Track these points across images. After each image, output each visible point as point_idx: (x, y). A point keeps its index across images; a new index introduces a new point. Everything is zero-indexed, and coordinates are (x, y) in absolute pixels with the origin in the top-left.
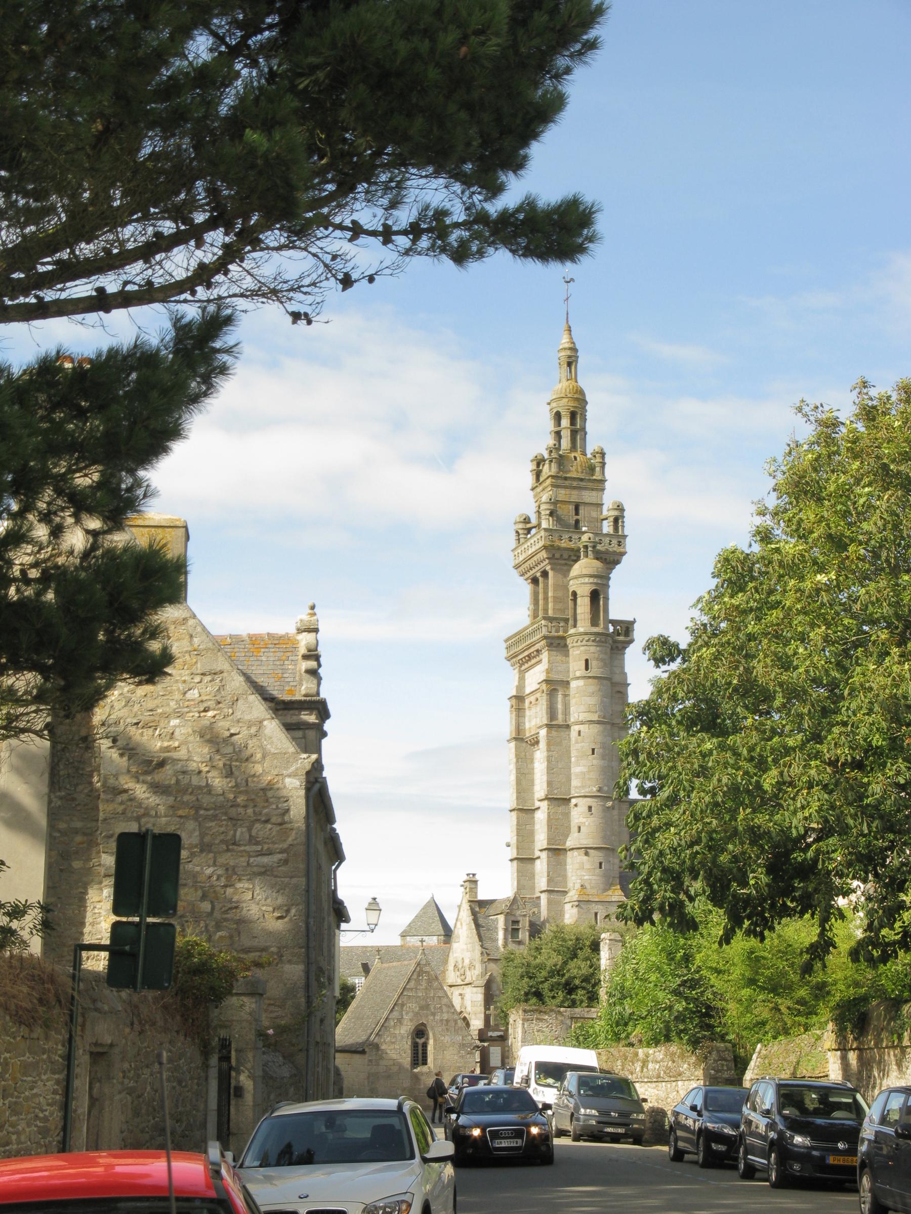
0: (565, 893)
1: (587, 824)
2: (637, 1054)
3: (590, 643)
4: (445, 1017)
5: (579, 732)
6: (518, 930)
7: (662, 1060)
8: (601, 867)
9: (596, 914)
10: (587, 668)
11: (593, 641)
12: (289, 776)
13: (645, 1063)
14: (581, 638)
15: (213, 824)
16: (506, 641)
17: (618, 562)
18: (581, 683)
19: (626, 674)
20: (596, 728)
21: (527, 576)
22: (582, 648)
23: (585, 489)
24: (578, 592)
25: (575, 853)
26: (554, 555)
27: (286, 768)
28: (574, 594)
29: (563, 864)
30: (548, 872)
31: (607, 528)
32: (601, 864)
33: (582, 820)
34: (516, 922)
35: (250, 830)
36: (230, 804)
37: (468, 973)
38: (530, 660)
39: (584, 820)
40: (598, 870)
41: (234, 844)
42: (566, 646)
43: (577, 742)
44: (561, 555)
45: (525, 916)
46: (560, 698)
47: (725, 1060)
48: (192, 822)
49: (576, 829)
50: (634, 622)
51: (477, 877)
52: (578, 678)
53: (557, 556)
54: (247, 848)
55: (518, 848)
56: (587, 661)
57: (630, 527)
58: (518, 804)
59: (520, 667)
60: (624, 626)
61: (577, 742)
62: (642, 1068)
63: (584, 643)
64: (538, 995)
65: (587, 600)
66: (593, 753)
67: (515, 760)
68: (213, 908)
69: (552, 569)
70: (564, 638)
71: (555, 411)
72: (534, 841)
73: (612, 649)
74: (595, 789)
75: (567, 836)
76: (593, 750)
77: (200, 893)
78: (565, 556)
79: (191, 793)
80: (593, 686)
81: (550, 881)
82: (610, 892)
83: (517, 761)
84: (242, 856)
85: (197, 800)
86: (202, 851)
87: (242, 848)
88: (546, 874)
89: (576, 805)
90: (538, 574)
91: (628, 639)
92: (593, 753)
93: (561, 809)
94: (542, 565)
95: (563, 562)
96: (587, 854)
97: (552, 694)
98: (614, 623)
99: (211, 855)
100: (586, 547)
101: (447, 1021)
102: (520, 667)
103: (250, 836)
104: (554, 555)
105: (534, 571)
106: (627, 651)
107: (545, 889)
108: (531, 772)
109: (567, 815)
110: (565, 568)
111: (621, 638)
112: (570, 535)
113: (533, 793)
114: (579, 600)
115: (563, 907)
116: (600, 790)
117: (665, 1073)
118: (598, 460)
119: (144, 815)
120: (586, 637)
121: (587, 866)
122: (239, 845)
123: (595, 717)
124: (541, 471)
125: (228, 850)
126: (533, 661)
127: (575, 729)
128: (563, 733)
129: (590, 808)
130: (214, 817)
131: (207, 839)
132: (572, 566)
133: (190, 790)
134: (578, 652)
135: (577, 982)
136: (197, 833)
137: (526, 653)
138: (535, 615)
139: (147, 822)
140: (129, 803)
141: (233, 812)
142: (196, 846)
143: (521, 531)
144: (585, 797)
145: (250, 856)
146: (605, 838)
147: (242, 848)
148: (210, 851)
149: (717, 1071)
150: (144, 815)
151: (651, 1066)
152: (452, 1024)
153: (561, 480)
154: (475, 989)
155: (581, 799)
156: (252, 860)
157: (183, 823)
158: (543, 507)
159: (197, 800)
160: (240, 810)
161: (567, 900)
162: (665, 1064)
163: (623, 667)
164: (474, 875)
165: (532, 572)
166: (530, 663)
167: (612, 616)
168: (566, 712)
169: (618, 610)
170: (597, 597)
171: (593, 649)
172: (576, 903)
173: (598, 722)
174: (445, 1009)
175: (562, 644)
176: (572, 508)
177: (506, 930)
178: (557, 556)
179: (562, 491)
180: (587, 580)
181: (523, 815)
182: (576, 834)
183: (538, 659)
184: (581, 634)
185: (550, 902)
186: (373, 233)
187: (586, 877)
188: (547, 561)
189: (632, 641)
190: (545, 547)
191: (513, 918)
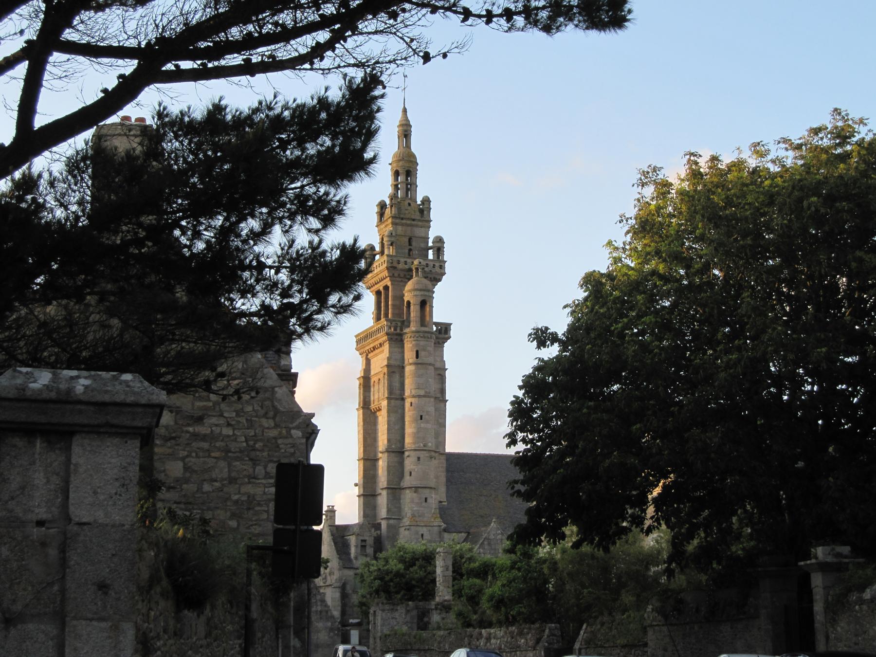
2: (481, 634)
4: (319, 608)
5: (411, 403)
7: (503, 637)
10: (417, 357)
12: (294, 428)
13: (488, 639)
15: (238, 463)
16: (356, 336)
17: (440, 280)
19: (444, 361)
21: (372, 289)
23: (417, 226)
24: (412, 302)
27: (292, 423)
28: (409, 303)
30: (388, 505)
31: (431, 256)
33: (412, 467)
35: (265, 467)
36: (251, 449)
37: (328, 578)
38: (374, 350)
39: (414, 467)
41: (255, 478)
44: (399, 275)
47: (555, 635)
48: (222, 462)
50: (450, 324)
51: (335, 508)
52: (411, 364)
53: (396, 275)
54: (263, 481)
56: (417, 352)
57: (448, 255)
60: (443, 327)
62: (486, 643)
64: (387, 592)
65: (418, 307)
68: (238, 525)
71: (395, 169)
73: (435, 343)
77: (228, 514)
78: (402, 275)
79: (222, 441)
84: (260, 487)
85: (227, 445)
86: (230, 483)
87: (260, 481)
89: (408, 456)
90: (381, 289)
91: (447, 336)
94: (385, 281)
95: (400, 279)
98: (437, 324)
99: (237, 486)
100: (417, 269)
101: (321, 612)
103: (266, 472)
106: (446, 344)
107: (385, 516)
110: (401, 284)
111: (442, 336)
112: (405, 260)
114: (412, 307)
117: (505, 646)
119: (187, 456)
121: (416, 500)
122: (258, 479)
124: (384, 213)
125: (249, 483)
126: (377, 351)
129: (419, 458)
130: (237, 459)
131: (233, 474)
132: (406, 283)
133: (221, 438)
135: (414, 582)
136: (226, 470)
137: (372, 345)
138: (378, 318)
139: (190, 461)
140: (176, 447)
141: (253, 454)
142: (225, 479)
144: (415, 450)
145: (265, 487)
147: (260, 481)
148: (236, 483)
149: (550, 644)
150: (187, 456)
151: (493, 641)
152: (324, 614)
153: (398, 219)
154: (334, 589)
155: (412, 452)
156: (267, 490)
157: (216, 463)
158: (385, 239)
159: (227, 445)
160: (258, 453)
162: (505, 640)
163: (443, 357)
164: (333, 506)
165: (376, 286)
166: (374, 352)
167: (434, 320)
169: (439, 315)
170: (425, 304)
174: (319, 603)
176: (407, 240)
177: (356, 546)
179: (400, 228)
183: (381, 349)
184: (413, 332)
186: (479, 16)
187: (415, 509)
189: (449, 338)
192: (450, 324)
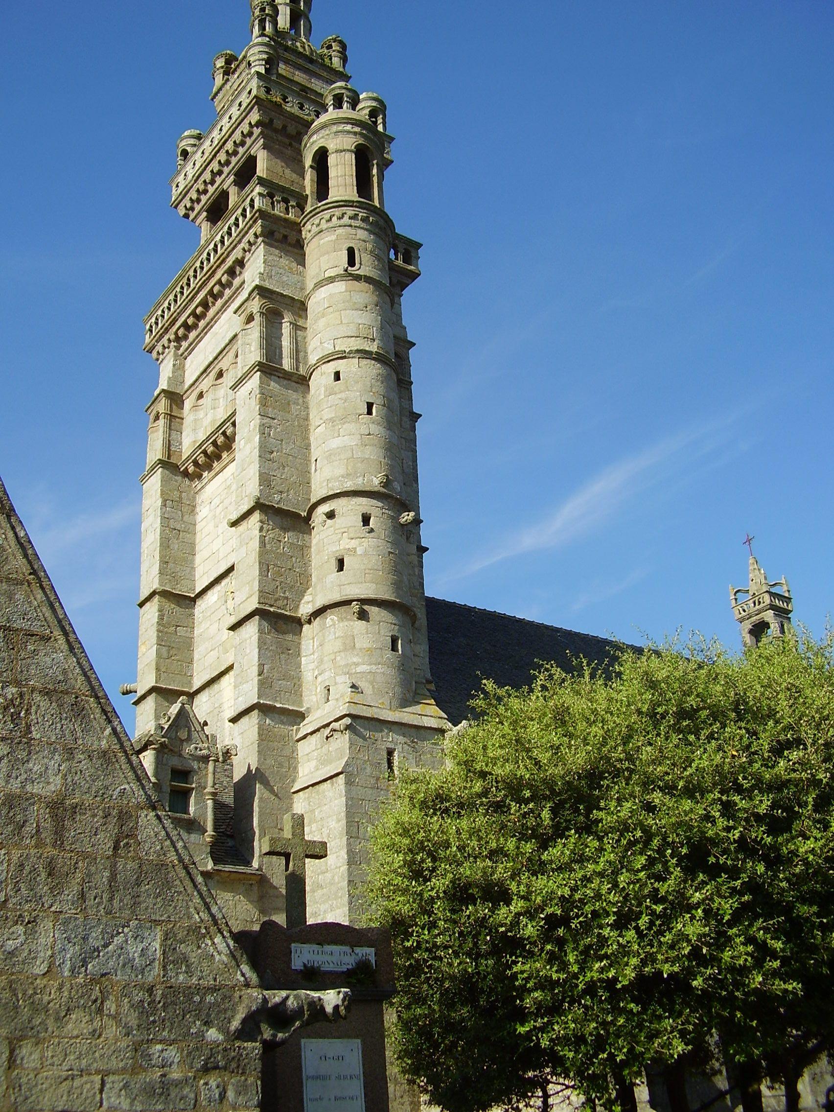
0: (299, 717)
1: (359, 551)
3: (358, 223)
6: (186, 793)
8: (394, 648)
9: (390, 753)
11: (364, 220)
14: (338, 212)
18: (340, 287)
20: (372, 369)
22: (340, 231)
24: (331, 146)
25: (331, 618)
26: (271, 121)
28: (322, 156)
29: (292, 653)
30: (261, 666)
32: (394, 640)
33: (346, 544)
34: (183, 774)
39: (353, 544)
40: (389, 654)
42: (299, 245)
43: (331, 393)
44: (285, 127)
45: (205, 759)
46: (286, 329)
49: (334, 564)
52: (332, 280)
53: (278, 124)
55: (158, 669)
56: (351, 252)
58: (161, 583)
59: (178, 348)
61: (331, 393)
63: (346, 220)
65: (350, 159)
66: (370, 412)
67: (159, 502)
69: (265, 147)
70: (297, 228)
72: (191, 662)
74: (376, 481)
75: (302, 594)
76: (370, 406)
80: (364, 294)
81: (264, 684)
82: (418, 708)
83: (164, 505)
88: (255, 670)
89: (331, 515)
92: (370, 412)
93: (288, 537)
95: (287, 141)
96: (363, 616)
97: (272, 317)
102: (178, 348)
104: (271, 121)
105: (219, 180)
108: (191, 529)
109: (303, 550)
113: (193, 569)
114: (332, 160)
115: (294, 750)
116: (387, 484)
118: (335, 47)
120: (350, 211)
121: (364, 642)
123: (374, 348)
127: (321, 380)
128: (292, 395)
129: (366, 520)
134: (334, 237)
143: (189, 149)
146: (397, 586)
155: (343, 501)
161: (306, 727)
168: (298, 352)
171: (362, 234)
172: (347, 721)
173: (378, 358)
175: (292, 238)
178: (278, 124)
180: (348, 127)
181: (169, 606)
182: (334, 576)
185: (264, 737)
187: (359, 669)
188: (257, 131)
190: (258, 101)
191: (175, 762)
192: (419, 245)
